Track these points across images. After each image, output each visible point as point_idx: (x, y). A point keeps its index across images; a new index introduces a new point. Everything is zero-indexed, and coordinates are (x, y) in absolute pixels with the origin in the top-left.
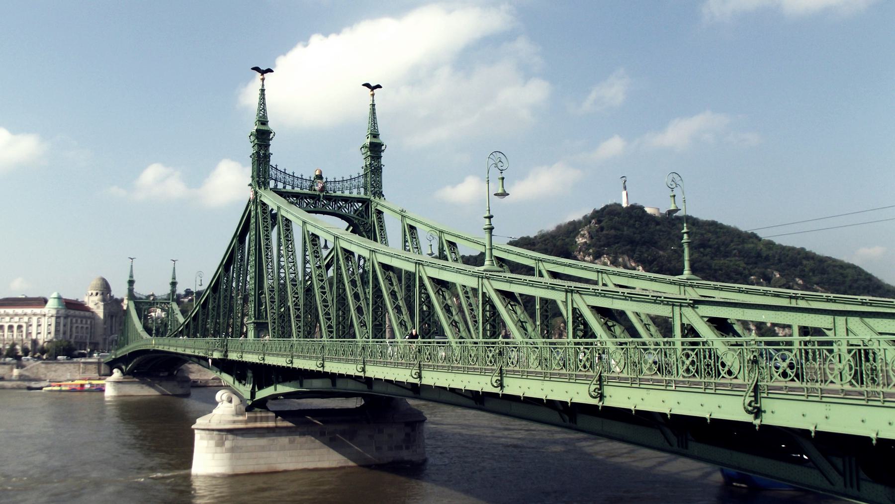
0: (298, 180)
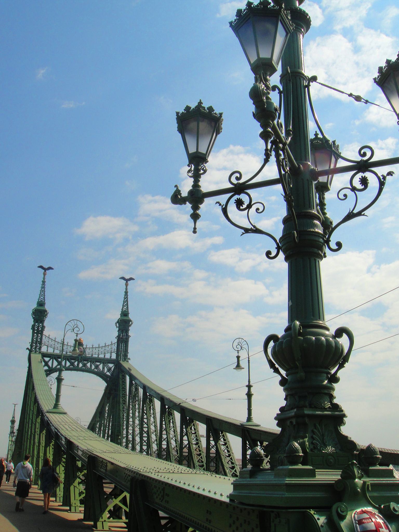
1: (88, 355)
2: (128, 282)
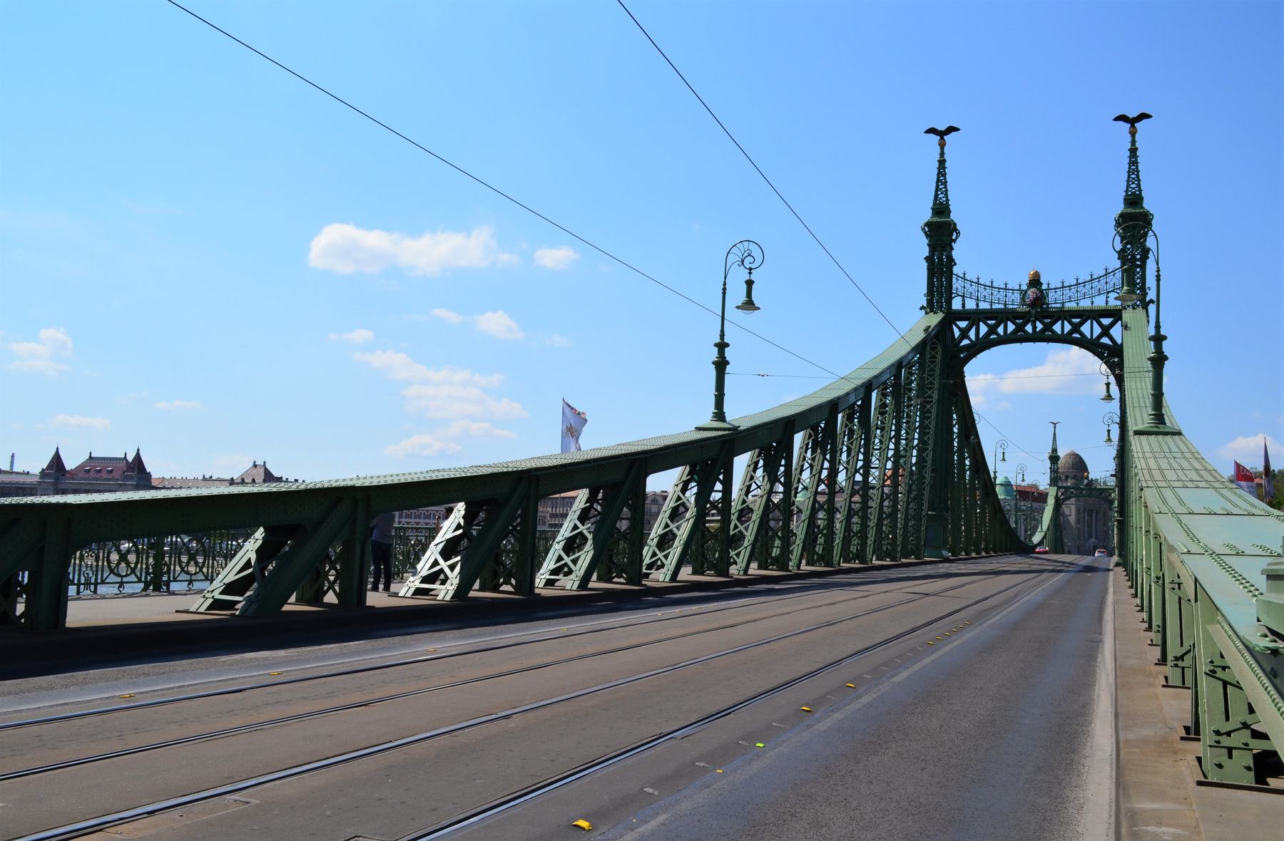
0: (999, 292)
1: (1053, 305)
2: (1136, 125)
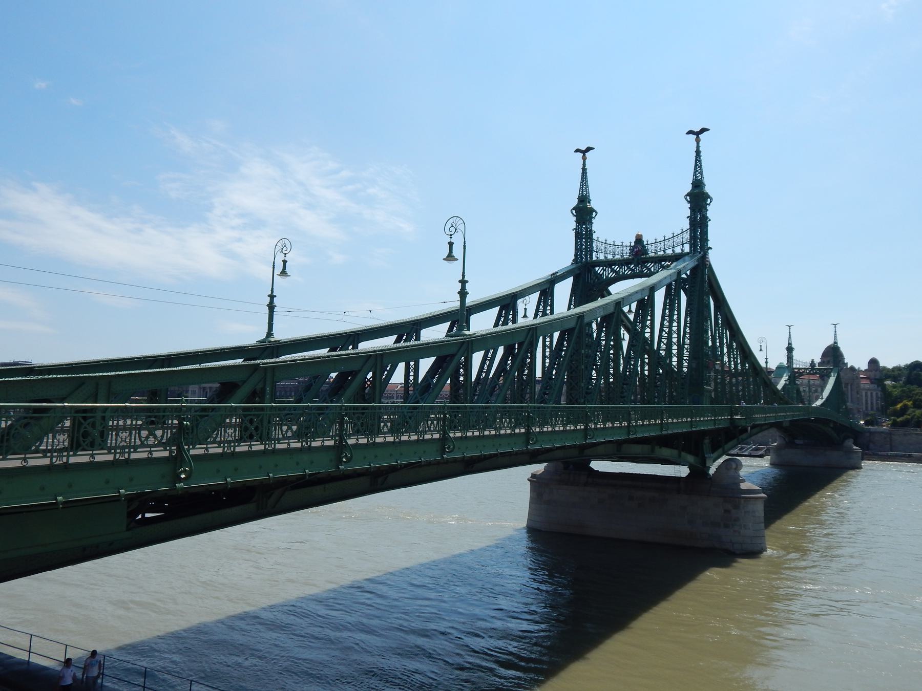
2: (700, 135)
